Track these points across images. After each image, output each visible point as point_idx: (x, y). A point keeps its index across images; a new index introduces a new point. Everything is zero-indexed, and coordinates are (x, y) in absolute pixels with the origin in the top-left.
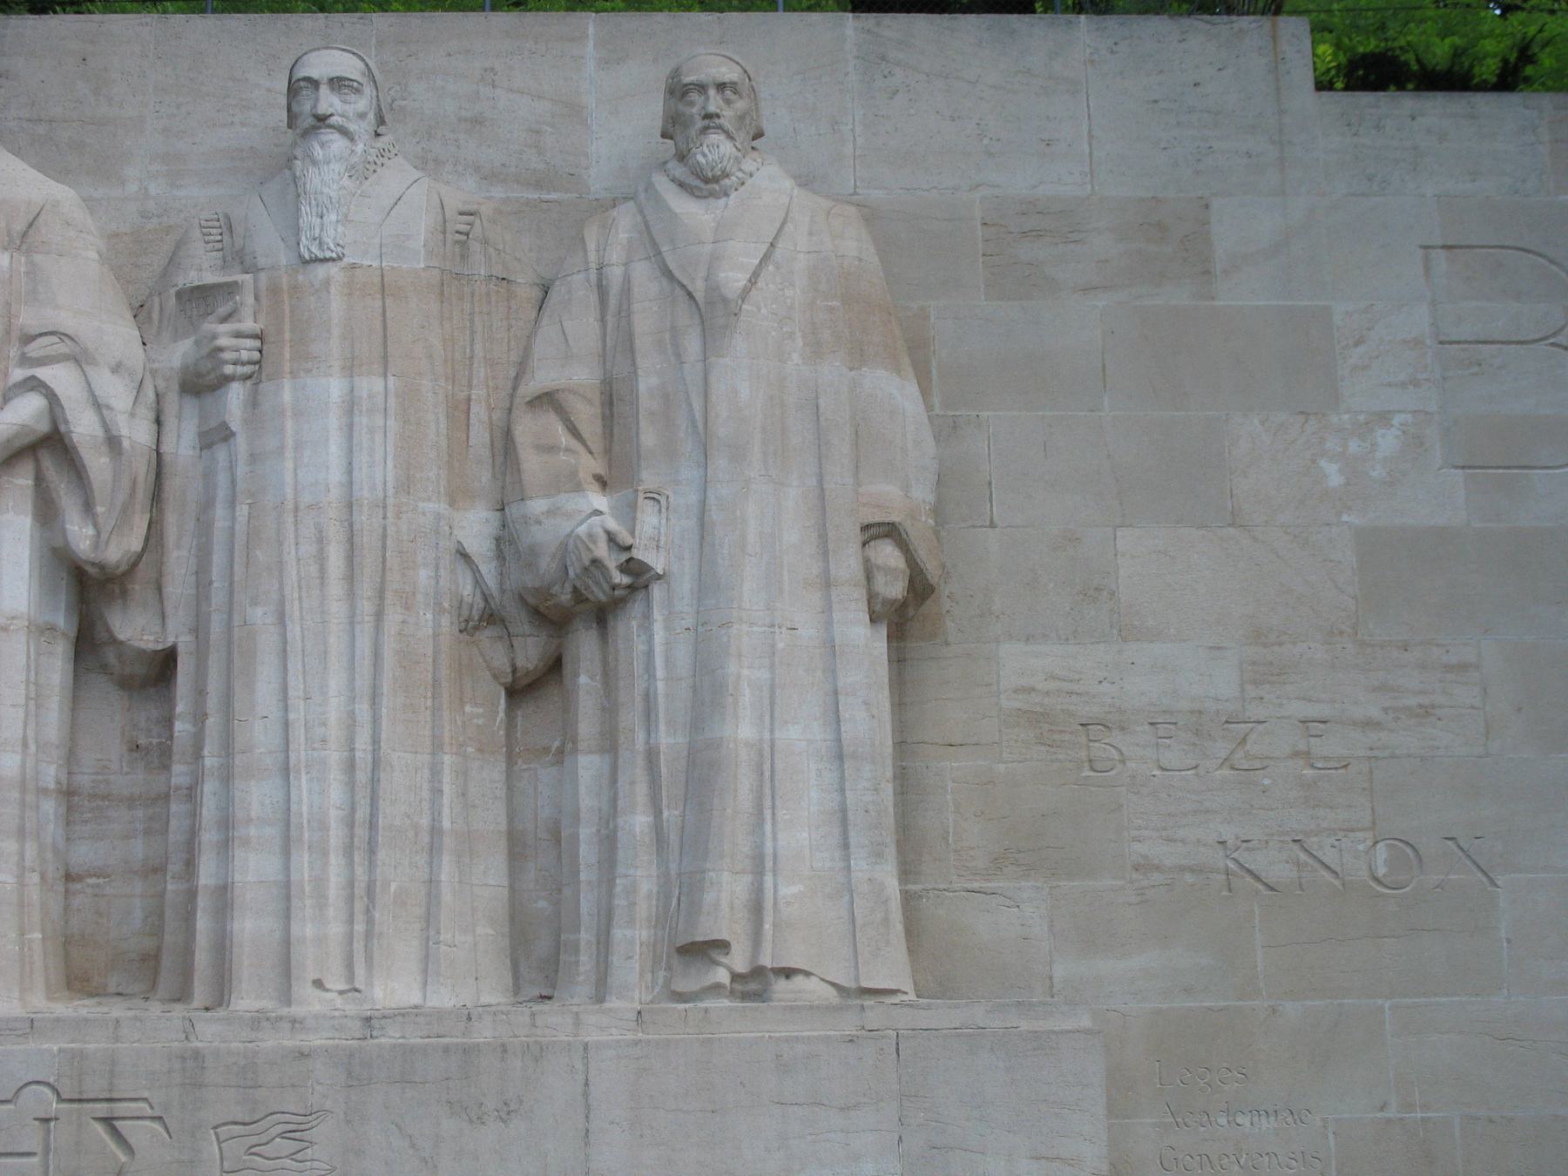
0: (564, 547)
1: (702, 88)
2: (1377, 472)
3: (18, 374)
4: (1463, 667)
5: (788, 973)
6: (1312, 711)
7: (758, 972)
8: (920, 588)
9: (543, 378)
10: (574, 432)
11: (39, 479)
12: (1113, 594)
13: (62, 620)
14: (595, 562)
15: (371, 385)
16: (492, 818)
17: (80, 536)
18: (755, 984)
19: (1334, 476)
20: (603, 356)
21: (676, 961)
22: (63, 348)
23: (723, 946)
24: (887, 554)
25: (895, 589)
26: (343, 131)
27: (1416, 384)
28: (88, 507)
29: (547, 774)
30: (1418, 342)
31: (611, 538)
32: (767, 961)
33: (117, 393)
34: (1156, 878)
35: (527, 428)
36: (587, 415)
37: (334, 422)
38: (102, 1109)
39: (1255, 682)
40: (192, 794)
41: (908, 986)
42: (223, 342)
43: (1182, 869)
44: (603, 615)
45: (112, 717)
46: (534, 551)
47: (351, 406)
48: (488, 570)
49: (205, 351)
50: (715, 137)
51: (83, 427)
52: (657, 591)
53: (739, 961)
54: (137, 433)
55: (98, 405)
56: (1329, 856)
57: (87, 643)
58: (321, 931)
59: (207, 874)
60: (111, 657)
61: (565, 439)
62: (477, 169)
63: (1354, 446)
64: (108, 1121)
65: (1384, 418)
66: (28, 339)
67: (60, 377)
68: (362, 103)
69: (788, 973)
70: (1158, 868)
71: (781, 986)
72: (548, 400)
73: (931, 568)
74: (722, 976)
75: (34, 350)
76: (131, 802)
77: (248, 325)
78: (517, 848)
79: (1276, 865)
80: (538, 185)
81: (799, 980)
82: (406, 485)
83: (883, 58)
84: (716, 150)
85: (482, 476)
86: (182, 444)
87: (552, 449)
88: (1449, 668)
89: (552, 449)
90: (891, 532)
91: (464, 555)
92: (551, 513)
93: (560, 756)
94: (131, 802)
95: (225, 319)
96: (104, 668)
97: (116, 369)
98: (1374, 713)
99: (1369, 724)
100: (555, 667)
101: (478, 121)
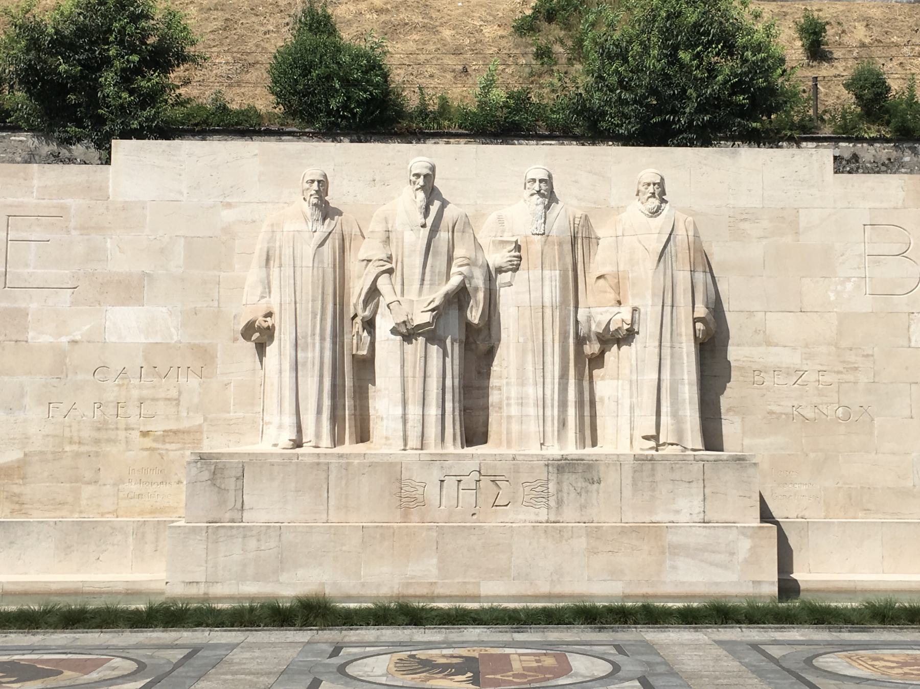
2: (846, 296)
4: (868, 356)
5: (672, 444)
6: (824, 368)
11: (459, 300)
12: (764, 332)
13: (464, 338)
14: (619, 328)
19: (832, 297)
22: (466, 262)
27: (859, 268)
30: (860, 255)
34: (774, 416)
39: (806, 359)
43: (782, 413)
60: (473, 347)
61: (609, 289)
62: (576, 197)
63: (839, 288)
65: (849, 279)
70: (774, 413)
79: (809, 413)
80: (595, 203)
82: (564, 302)
83: (700, 162)
88: (863, 356)
89: (606, 292)
92: (606, 312)
95: (510, 251)
98: (841, 369)
99: (839, 372)
101: (576, 182)
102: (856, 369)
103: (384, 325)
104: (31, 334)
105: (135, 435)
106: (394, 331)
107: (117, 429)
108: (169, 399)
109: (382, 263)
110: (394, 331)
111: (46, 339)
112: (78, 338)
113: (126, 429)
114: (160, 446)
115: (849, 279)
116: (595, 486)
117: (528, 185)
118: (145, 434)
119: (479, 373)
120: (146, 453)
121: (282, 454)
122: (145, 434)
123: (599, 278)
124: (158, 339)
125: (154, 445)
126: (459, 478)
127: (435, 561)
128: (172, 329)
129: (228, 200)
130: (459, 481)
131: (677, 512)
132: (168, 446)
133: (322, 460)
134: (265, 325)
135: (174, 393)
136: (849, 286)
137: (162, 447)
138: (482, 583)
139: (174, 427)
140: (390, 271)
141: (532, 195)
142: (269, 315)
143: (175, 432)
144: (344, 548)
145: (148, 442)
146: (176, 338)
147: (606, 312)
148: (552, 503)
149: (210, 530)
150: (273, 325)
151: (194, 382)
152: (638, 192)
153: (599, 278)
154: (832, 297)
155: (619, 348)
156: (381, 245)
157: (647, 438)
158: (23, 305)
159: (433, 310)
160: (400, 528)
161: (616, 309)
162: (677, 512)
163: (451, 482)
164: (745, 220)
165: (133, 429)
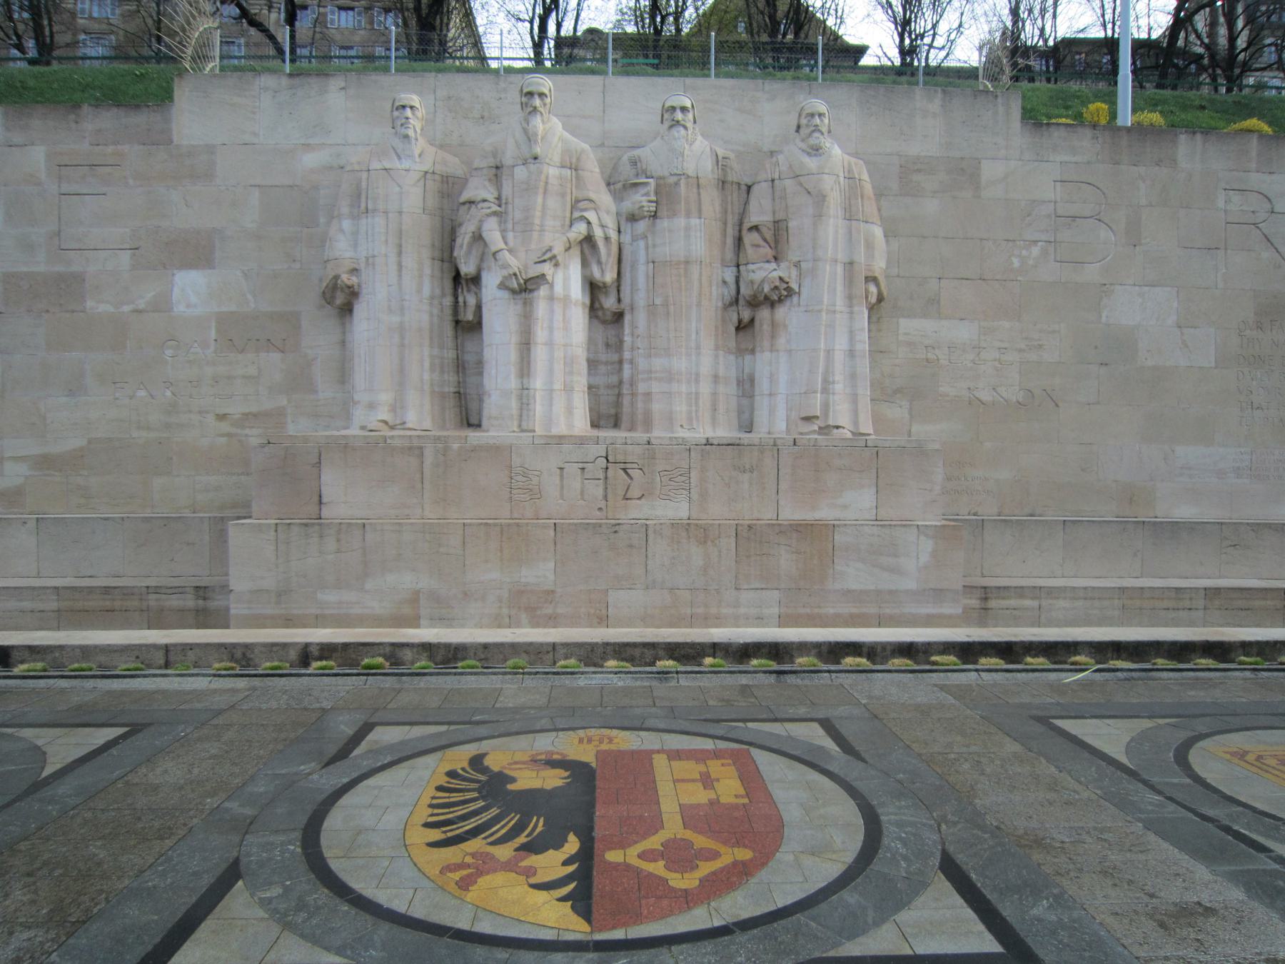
0: (763, 281)
1: (812, 115)
2: (1031, 262)
3: (576, 214)
4: (1054, 332)
5: (838, 427)
7: (828, 427)
8: (880, 299)
9: (754, 218)
10: (765, 240)
11: (582, 252)
13: (588, 302)
15: (695, 221)
16: (733, 373)
17: (597, 274)
18: (826, 430)
19: (1016, 262)
20: (774, 213)
21: (800, 422)
23: (817, 417)
24: (873, 289)
25: (873, 300)
26: (685, 128)
28: (599, 263)
29: (748, 358)
30: (1049, 216)
31: (781, 278)
32: (831, 422)
33: (611, 222)
35: (750, 238)
36: (769, 235)
37: (682, 233)
38: (622, 466)
40: (631, 362)
41: (871, 432)
42: (645, 204)
44: (773, 305)
45: (601, 333)
46: (752, 282)
47: (687, 229)
48: (733, 287)
49: (637, 206)
50: (816, 135)
51: (598, 233)
52: (795, 299)
53: (820, 423)
54: (613, 235)
55: (603, 226)
56: (1004, 394)
57: (594, 309)
58: (681, 408)
59: (642, 388)
60: (600, 313)
63: (1024, 253)
64: (624, 470)
65: (1035, 242)
66: (578, 201)
67: (591, 216)
68: (690, 116)
69: (838, 427)
71: (835, 431)
72: (755, 228)
73: (885, 294)
74: (816, 428)
75: (581, 205)
76: (606, 363)
77: (654, 198)
78: (740, 383)
81: (841, 430)
84: (816, 139)
85: (730, 255)
86: (626, 238)
87: (758, 246)
89: (758, 246)
90: (872, 279)
91: (724, 282)
93: (753, 352)
94: (606, 363)
96: (597, 317)
97: (608, 212)
98: (1023, 346)
99: (1021, 351)
100: (752, 321)
102: (1040, 346)
103: (490, 281)
104: (90, 304)
105: (210, 419)
106: (503, 286)
107: (190, 412)
108: (244, 377)
109: (486, 204)
110: (503, 286)
111: (103, 308)
112: (142, 306)
113: (200, 412)
114: (239, 431)
115: (1035, 242)
116: (746, 476)
117: (666, 116)
118: (222, 417)
119: (608, 345)
120: (223, 440)
121: (365, 437)
122: (222, 417)
123: (751, 229)
124: (233, 308)
125: (234, 430)
126: (581, 465)
127: (552, 565)
128: (250, 297)
129: (311, 141)
130: (583, 469)
131: (845, 507)
132: (247, 431)
133: (416, 443)
134: (349, 283)
135: (252, 371)
136: (1036, 251)
137: (239, 431)
138: (610, 592)
139: (254, 409)
140: (495, 213)
141: (671, 127)
142: (354, 271)
143: (255, 415)
144: (441, 550)
145: (225, 427)
146: (253, 305)
147: (760, 268)
148: (695, 496)
149: (280, 528)
150: (359, 286)
151: (276, 356)
152: (799, 127)
153: (751, 229)
154: (1016, 262)
155: (772, 314)
156: (487, 183)
157: (807, 419)
158: (75, 268)
159: (551, 259)
160: (509, 525)
161: (773, 265)
162: (845, 507)
163: (573, 469)
164: (919, 171)
165: (207, 412)
